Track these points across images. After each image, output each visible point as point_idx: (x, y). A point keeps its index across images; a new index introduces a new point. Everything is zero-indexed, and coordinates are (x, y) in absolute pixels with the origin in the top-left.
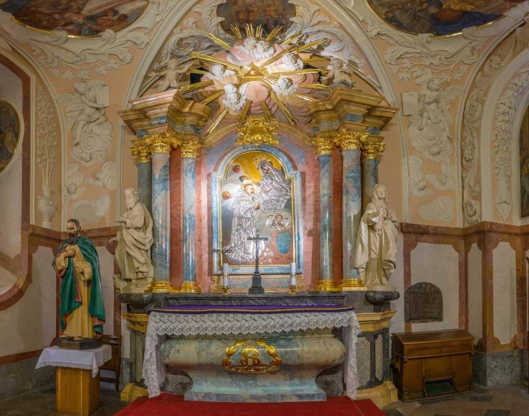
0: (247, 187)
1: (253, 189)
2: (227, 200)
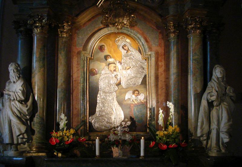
0: (110, 65)
1: (115, 67)
2: (94, 76)
